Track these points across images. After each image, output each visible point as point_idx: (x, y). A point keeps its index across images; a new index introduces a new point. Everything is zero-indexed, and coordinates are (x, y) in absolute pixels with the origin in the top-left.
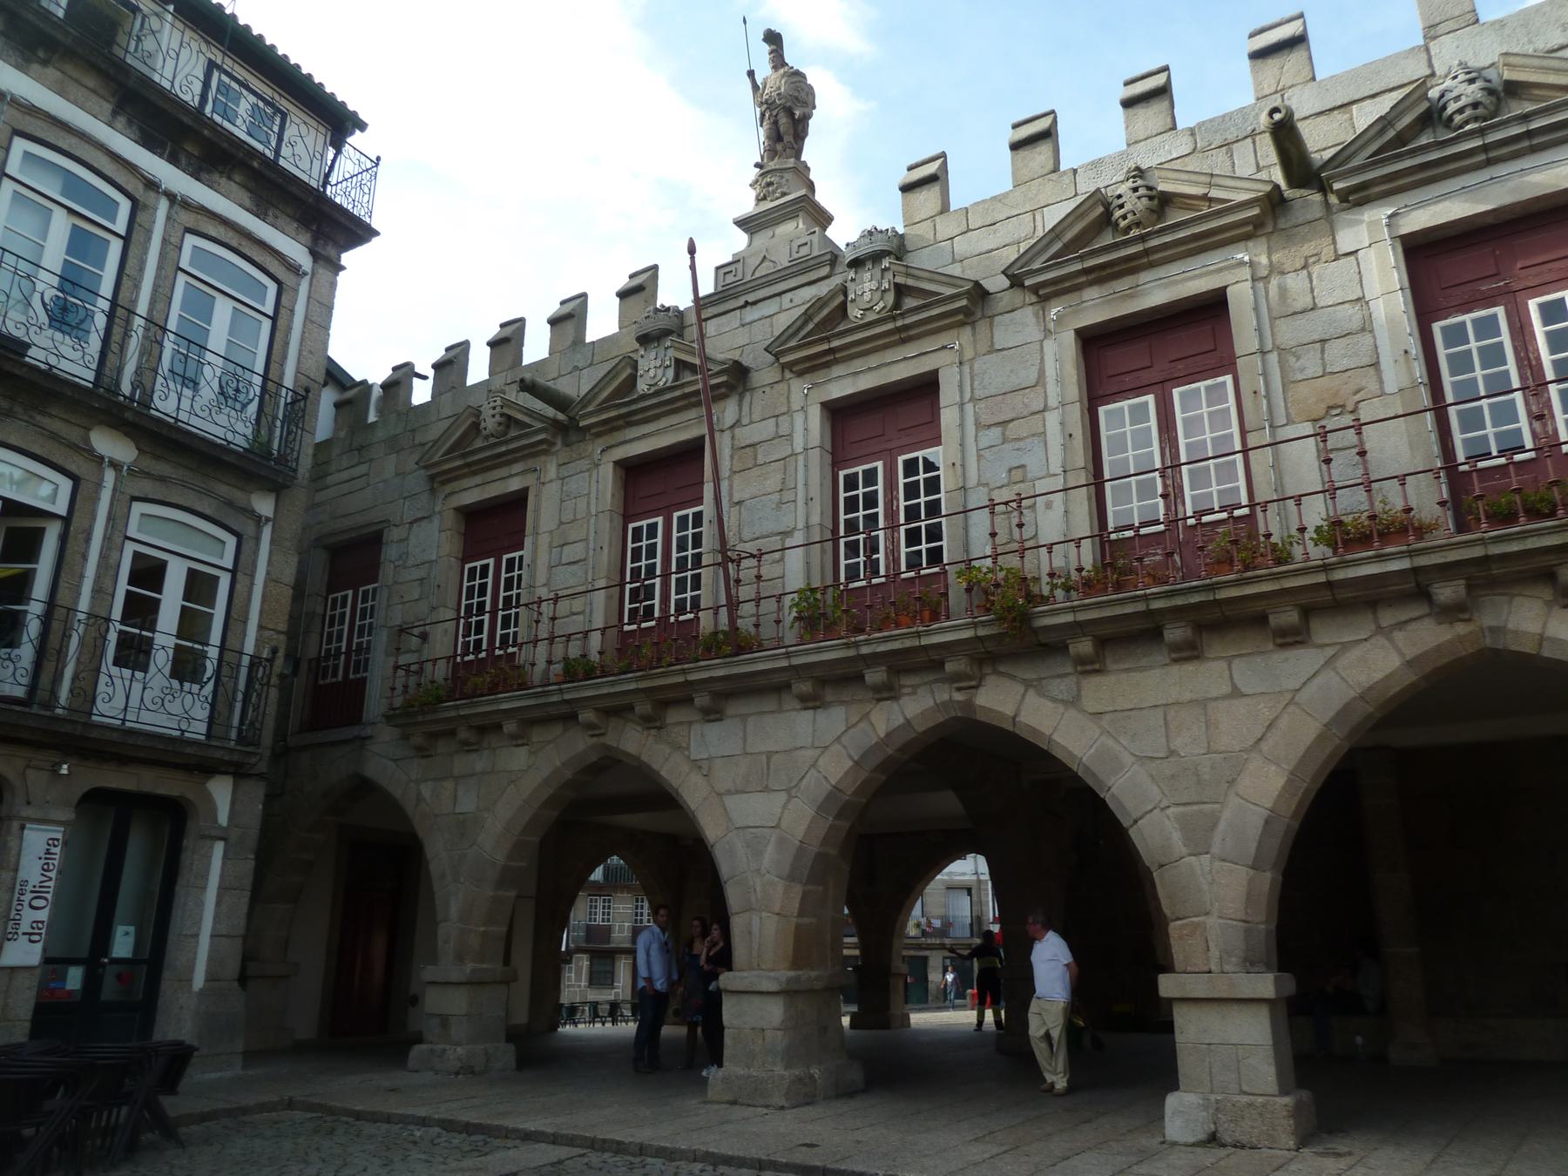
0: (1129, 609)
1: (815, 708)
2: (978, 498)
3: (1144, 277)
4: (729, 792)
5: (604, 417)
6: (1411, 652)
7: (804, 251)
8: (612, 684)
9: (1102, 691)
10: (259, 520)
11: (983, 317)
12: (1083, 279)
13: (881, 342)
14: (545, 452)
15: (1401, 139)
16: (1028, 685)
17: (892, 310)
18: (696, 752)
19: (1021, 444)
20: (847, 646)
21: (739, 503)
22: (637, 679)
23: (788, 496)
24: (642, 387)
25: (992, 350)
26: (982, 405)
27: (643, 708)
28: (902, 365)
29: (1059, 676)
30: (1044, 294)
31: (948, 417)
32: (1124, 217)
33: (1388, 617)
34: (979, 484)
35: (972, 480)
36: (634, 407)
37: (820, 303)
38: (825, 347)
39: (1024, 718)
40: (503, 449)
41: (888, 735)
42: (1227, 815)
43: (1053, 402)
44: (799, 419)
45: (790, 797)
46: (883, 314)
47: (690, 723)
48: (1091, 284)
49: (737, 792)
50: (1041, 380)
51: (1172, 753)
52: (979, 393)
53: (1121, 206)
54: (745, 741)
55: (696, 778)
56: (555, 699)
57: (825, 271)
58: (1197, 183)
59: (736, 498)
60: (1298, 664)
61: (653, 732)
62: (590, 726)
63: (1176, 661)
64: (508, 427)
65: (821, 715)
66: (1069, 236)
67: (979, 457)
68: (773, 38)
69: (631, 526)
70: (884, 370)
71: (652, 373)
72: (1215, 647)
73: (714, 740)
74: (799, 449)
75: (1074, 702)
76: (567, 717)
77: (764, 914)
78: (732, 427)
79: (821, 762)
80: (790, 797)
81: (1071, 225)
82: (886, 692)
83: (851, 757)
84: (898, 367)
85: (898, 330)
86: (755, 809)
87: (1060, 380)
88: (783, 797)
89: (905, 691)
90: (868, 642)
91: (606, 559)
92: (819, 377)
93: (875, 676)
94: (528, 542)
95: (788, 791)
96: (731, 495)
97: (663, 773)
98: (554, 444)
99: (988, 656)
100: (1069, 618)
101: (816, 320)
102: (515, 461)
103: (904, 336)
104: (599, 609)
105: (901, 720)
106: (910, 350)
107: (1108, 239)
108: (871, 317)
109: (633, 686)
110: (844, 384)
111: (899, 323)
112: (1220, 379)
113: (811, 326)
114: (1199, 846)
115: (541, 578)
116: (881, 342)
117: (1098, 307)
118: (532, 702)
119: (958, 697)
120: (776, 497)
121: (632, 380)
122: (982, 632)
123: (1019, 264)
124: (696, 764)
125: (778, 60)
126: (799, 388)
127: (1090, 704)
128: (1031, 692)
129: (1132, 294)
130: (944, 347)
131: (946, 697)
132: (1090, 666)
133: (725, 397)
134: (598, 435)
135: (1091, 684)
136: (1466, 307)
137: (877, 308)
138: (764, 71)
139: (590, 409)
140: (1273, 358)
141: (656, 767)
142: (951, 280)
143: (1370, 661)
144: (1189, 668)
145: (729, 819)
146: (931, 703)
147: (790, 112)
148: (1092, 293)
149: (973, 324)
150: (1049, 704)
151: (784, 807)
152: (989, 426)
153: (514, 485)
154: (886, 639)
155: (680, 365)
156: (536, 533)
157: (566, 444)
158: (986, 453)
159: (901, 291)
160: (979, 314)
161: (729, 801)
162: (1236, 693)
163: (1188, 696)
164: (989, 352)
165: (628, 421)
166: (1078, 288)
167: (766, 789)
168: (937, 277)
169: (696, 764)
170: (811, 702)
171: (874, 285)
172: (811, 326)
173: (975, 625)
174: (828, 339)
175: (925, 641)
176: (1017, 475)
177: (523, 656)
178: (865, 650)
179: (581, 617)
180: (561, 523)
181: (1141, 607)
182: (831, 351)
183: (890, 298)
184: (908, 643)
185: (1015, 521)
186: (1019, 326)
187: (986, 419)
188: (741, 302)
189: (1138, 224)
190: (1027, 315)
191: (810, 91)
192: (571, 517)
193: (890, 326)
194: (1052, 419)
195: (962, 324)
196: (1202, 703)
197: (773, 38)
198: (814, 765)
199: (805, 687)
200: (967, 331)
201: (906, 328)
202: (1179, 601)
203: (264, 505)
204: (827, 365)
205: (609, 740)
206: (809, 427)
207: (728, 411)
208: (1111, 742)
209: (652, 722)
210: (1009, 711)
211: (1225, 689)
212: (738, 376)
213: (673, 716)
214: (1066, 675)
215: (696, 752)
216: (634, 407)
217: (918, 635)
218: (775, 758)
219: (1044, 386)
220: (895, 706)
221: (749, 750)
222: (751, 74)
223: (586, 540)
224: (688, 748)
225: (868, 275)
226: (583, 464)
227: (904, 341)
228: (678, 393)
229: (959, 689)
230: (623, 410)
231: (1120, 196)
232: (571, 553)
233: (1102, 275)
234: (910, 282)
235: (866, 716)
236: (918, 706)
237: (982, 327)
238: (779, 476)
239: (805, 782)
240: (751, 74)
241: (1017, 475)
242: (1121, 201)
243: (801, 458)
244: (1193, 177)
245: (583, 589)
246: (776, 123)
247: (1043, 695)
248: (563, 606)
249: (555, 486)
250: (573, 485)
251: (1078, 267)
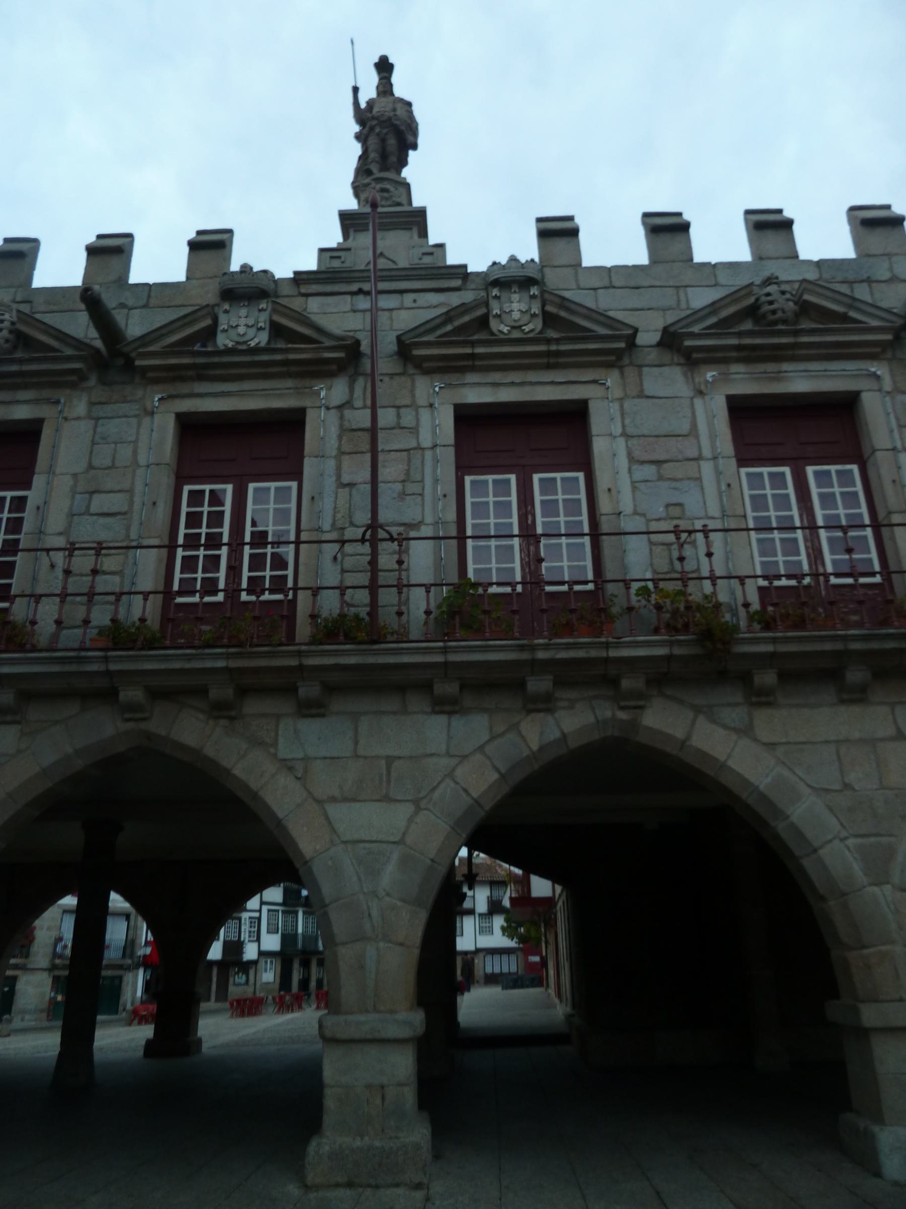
0: (828, 646)
1: (450, 713)
3: (785, 366)
4: (333, 799)
5: (173, 361)
7: (427, 260)
8: (189, 658)
9: (770, 723)
11: (631, 364)
12: (734, 354)
13: (527, 361)
14: (73, 386)
16: (697, 710)
17: (541, 332)
18: (285, 750)
19: (677, 485)
20: (522, 648)
21: (351, 485)
22: (228, 656)
23: (411, 488)
24: (223, 341)
25: (641, 395)
26: (635, 441)
27: (220, 692)
28: (548, 388)
29: (729, 705)
31: (599, 446)
32: (774, 312)
34: (635, 513)
36: (216, 360)
37: (464, 308)
38: (468, 350)
39: (697, 741)
40: (14, 368)
41: (541, 749)
43: (707, 452)
44: (425, 416)
45: (418, 809)
46: (531, 335)
47: (278, 717)
48: (738, 360)
49: (345, 800)
50: (693, 431)
51: (847, 786)
52: (630, 430)
53: (771, 303)
54: (356, 743)
55: (284, 780)
56: (94, 667)
57: (457, 283)
58: (839, 302)
59: (346, 479)
61: (223, 722)
62: (131, 708)
63: (842, 702)
64: (15, 347)
65: (458, 722)
66: (724, 313)
67: (634, 489)
68: (384, 67)
69: (187, 488)
70: (527, 388)
71: (242, 330)
73: (314, 739)
74: (426, 442)
75: (746, 731)
76: (102, 693)
77: (382, 944)
78: (340, 407)
79: (459, 772)
80: (418, 809)
81: (726, 306)
82: (543, 704)
83: (497, 770)
84: (545, 389)
85: (549, 354)
86: (373, 820)
87: (713, 437)
88: (410, 808)
89: (561, 704)
90: (546, 647)
91: (162, 512)
92: (454, 378)
93: (538, 684)
94: (38, 481)
95: (416, 802)
96: (339, 476)
97: (237, 772)
98: (82, 377)
99: (664, 677)
100: (770, 648)
101: (457, 323)
102: (25, 387)
103: (551, 361)
104: (147, 569)
105: (557, 734)
107: (748, 325)
108: (516, 334)
109: (221, 664)
110: (479, 392)
111: (553, 348)
112: (848, 467)
113: (449, 328)
114: (881, 878)
115: (56, 521)
116: (527, 361)
117: (746, 382)
118: (56, 668)
119: (622, 715)
120: (398, 487)
121: (211, 332)
122: (677, 651)
123: (680, 325)
124: (287, 766)
125: (385, 87)
126: (425, 387)
128: (701, 719)
129: (777, 377)
130: (595, 382)
131: (608, 714)
132: (760, 698)
133: (332, 375)
134: (156, 381)
135: (762, 716)
137: (527, 329)
138: (368, 93)
139: (151, 348)
141: (225, 763)
142: (611, 323)
144: (856, 709)
145: (334, 830)
146: (592, 719)
148: (737, 368)
149: (621, 368)
150: (721, 732)
151: (410, 820)
152: (643, 462)
153: (22, 413)
154: (568, 647)
155: (277, 330)
156: (51, 471)
157: (103, 382)
158: (642, 486)
160: (626, 361)
161: (331, 809)
163: (857, 735)
164: (639, 397)
165: (201, 373)
166: (726, 361)
167: (387, 799)
168: (594, 315)
169: (287, 766)
170: (446, 706)
171: (524, 307)
172: (449, 328)
173: (671, 644)
174: (473, 344)
175: (613, 653)
176: (675, 512)
177: (19, 610)
178: (541, 655)
179: (117, 579)
180: (91, 467)
181: (839, 646)
182: (473, 356)
184: (593, 653)
185: (676, 554)
186: (668, 380)
187: (638, 454)
188: (354, 287)
189: (784, 321)
192: (108, 462)
193: (542, 348)
195: (609, 365)
197: (384, 67)
198: (450, 775)
199: (451, 688)
200: (615, 373)
201: (558, 354)
202: (875, 645)
204: (462, 370)
205: (156, 725)
206: (438, 425)
207: (335, 391)
208: (786, 773)
209: (222, 710)
210: (679, 734)
211: (891, 731)
212: (349, 358)
213: (252, 706)
214: (736, 705)
215: (285, 750)
216: (216, 360)
217: (607, 646)
218: (397, 764)
219: (697, 437)
220: (550, 719)
221: (361, 752)
222: (356, 90)
223: (131, 491)
224: (275, 744)
225: (515, 297)
226: (125, 408)
227: (548, 367)
228: (278, 357)
229: (622, 708)
230: (201, 360)
231: (768, 294)
232: (99, 503)
233: (750, 355)
234: (563, 314)
235: (514, 727)
236: (575, 721)
237: (630, 372)
238: (402, 467)
239: (437, 794)
240: (356, 90)
241: (675, 512)
242: (769, 298)
243: (428, 454)
244: (837, 297)
245: (124, 544)
246: (383, 141)
247: (714, 721)
248: (110, 563)
249: (85, 426)
250: (111, 428)
251: (734, 341)
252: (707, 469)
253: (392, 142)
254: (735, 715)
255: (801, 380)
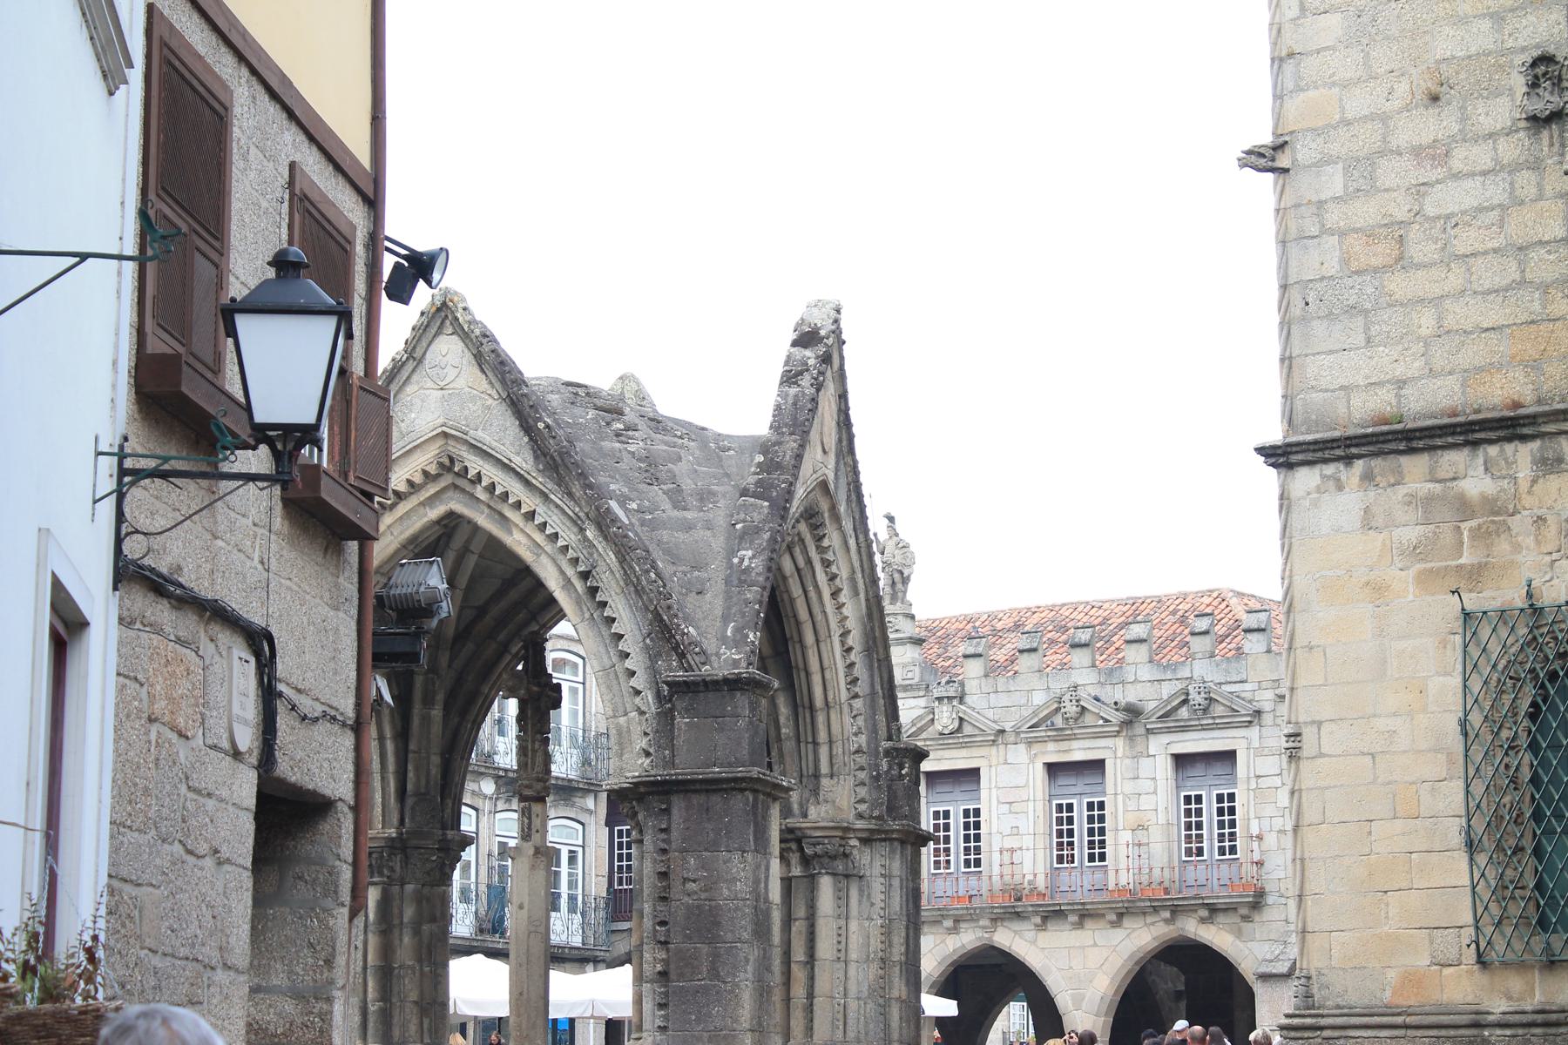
2: (996, 848)
6: (1155, 934)
7: (910, 675)
10: (590, 812)
15: (1176, 709)
16: (1016, 932)
30: (1030, 743)
31: (984, 793)
33: (1149, 919)
35: (994, 830)
37: (920, 718)
42: (1088, 995)
60: (1118, 935)
72: (1089, 924)
75: (1034, 942)
82: (954, 930)
106: (964, 753)
127: (1040, 943)
135: (1041, 935)
136: (1192, 788)
140: (1120, 798)
143: (1142, 937)
144: (1079, 932)
147: (901, 573)
148: (1051, 746)
159: (961, 719)
162: (1095, 945)
183: (956, 724)
186: (1019, 753)
190: (1022, 747)
191: (909, 561)
194: (1031, 804)
196: (1083, 948)
200: (994, 749)
203: (590, 802)
252: (1031, 804)
253: (897, 576)
254: (1030, 935)
255: (1079, 752)
